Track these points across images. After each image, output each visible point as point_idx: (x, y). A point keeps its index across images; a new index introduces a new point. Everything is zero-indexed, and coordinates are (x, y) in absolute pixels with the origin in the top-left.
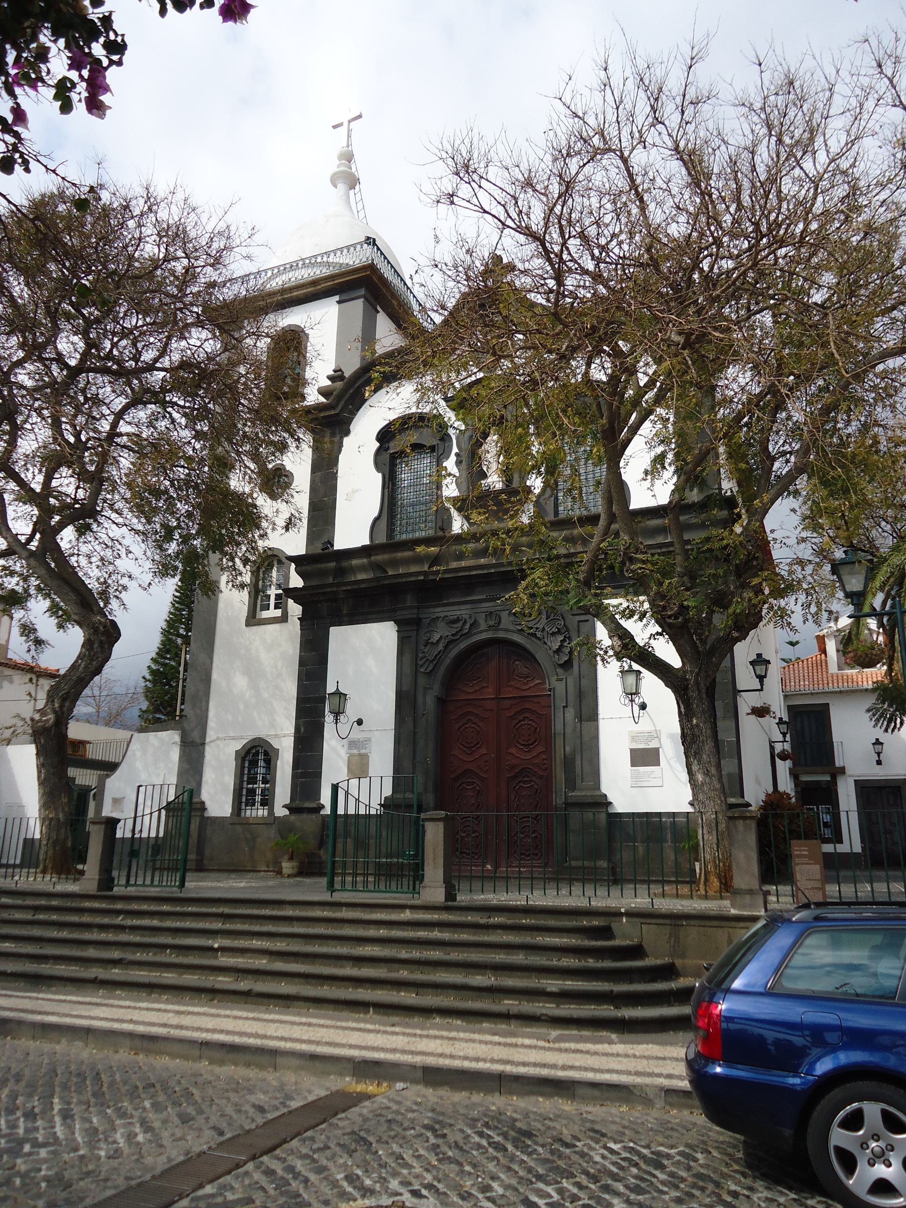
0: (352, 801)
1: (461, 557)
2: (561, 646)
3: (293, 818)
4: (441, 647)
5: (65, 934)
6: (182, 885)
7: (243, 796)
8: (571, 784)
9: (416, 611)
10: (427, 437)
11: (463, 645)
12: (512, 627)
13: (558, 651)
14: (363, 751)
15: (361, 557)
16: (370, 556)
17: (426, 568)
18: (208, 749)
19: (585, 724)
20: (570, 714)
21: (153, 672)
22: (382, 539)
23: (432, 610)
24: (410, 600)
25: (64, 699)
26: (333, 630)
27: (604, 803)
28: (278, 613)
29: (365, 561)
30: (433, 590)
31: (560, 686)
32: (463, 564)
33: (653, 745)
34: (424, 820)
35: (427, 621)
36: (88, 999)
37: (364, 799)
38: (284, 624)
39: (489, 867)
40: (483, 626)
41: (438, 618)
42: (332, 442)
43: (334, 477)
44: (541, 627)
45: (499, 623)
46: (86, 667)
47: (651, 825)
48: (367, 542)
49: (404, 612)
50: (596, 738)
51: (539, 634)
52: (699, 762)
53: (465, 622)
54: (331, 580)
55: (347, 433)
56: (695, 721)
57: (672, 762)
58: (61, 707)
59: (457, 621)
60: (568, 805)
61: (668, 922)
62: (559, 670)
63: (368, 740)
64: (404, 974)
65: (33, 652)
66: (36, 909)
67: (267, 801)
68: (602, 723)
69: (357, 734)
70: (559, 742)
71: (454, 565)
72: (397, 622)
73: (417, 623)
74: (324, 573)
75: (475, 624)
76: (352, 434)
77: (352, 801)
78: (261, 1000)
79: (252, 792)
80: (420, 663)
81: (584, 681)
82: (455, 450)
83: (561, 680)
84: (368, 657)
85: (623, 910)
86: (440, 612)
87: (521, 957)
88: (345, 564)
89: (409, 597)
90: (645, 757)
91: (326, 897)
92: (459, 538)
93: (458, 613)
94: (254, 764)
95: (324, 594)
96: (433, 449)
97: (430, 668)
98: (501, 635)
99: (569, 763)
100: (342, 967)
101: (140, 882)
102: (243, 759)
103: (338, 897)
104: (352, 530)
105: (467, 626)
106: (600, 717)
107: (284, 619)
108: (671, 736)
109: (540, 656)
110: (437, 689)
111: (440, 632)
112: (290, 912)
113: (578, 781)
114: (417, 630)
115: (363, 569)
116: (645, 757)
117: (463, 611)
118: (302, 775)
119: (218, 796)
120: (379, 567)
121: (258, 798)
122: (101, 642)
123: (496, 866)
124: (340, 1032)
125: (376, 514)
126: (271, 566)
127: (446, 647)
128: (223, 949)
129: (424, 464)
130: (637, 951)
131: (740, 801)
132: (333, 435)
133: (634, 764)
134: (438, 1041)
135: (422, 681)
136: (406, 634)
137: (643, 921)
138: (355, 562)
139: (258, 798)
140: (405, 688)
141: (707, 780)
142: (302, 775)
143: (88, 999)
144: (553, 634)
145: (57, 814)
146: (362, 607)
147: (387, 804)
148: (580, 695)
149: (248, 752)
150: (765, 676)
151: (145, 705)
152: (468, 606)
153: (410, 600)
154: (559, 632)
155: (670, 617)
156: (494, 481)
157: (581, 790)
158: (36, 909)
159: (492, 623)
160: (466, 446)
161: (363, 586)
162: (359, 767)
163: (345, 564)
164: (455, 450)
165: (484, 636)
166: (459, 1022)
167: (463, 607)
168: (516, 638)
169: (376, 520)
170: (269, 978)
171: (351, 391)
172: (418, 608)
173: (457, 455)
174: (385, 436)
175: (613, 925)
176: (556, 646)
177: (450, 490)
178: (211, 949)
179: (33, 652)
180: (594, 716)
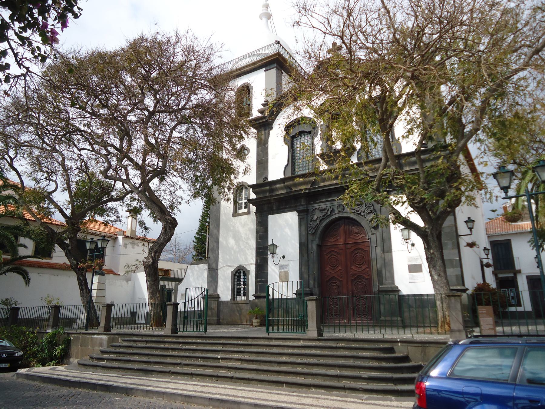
0: (275, 293)
1: (324, 180)
3: (257, 301)
4: (318, 221)
5: (158, 352)
6: (206, 331)
7: (235, 292)
8: (381, 282)
11: (328, 220)
14: (286, 270)
15: (281, 184)
16: (284, 183)
17: (309, 186)
18: (219, 271)
19: (386, 254)
20: (379, 249)
21: (197, 239)
22: (289, 175)
23: (313, 205)
24: (303, 202)
25: (155, 253)
26: (270, 217)
27: (396, 290)
28: (246, 210)
29: (282, 185)
30: (314, 196)
31: (373, 237)
32: (326, 184)
33: (419, 262)
34: (307, 300)
36: (166, 380)
37: (280, 291)
40: (337, 211)
44: (363, 210)
46: (164, 238)
47: (420, 301)
48: (283, 177)
49: (301, 207)
50: (391, 260)
51: (362, 214)
52: (435, 270)
53: (328, 210)
54: (268, 195)
55: (272, 128)
56: (432, 251)
58: (155, 256)
59: (325, 209)
60: (380, 292)
61: (420, 345)
62: (373, 230)
63: (288, 265)
64: (299, 369)
65: (144, 233)
66: (147, 342)
67: (246, 293)
68: (394, 254)
69: (283, 262)
70: (374, 263)
71: (322, 184)
73: (307, 211)
74: (264, 192)
75: (333, 211)
76: (274, 129)
77: (275, 293)
78: (237, 380)
79: (239, 290)
80: (309, 229)
81: (384, 234)
82: (320, 132)
83: (374, 234)
84: (286, 227)
85: (399, 340)
86: (317, 206)
87: (351, 362)
88: (273, 187)
89: (302, 200)
90: (414, 268)
91: (266, 335)
94: (239, 277)
95: (265, 201)
96: (309, 133)
97: (314, 231)
98: (345, 215)
99: (379, 273)
100: (272, 366)
101: (188, 330)
102: (235, 275)
103: (271, 335)
104: (276, 171)
105: (329, 212)
106: (393, 250)
107: (249, 213)
111: (317, 215)
112: (250, 342)
113: (384, 280)
115: (281, 188)
117: (327, 205)
118: (260, 282)
119: (225, 292)
121: (242, 292)
122: (170, 228)
124: (269, 395)
125: (286, 164)
126: (242, 189)
127: (320, 222)
128: (222, 359)
129: (306, 139)
130: (406, 359)
131: (462, 288)
132: (265, 130)
133: (410, 271)
134: (312, 399)
135: (310, 237)
136: (302, 217)
137: (409, 345)
138: (278, 186)
139: (242, 292)
140: (303, 241)
141: (440, 278)
142: (260, 282)
143: (166, 380)
144: (369, 213)
145: (155, 302)
146: (282, 204)
147: (298, 293)
148: (383, 240)
149: (236, 272)
150: (472, 228)
151: (194, 253)
152: (329, 203)
153: (303, 202)
154: (371, 212)
155: (416, 203)
157: (385, 284)
158: (147, 342)
159: (340, 210)
161: (282, 196)
162: (284, 277)
163: (273, 187)
164: (320, 132)
166: (323, 391)
167: (327, 203)
168: (352, 216)
169: (286, 166)
170: (241, 371)
174: (287, 128)
175: (395, 347)
177: (318, 150)
178: (217, 358)
179: (144, 233)
180: (390, 250)
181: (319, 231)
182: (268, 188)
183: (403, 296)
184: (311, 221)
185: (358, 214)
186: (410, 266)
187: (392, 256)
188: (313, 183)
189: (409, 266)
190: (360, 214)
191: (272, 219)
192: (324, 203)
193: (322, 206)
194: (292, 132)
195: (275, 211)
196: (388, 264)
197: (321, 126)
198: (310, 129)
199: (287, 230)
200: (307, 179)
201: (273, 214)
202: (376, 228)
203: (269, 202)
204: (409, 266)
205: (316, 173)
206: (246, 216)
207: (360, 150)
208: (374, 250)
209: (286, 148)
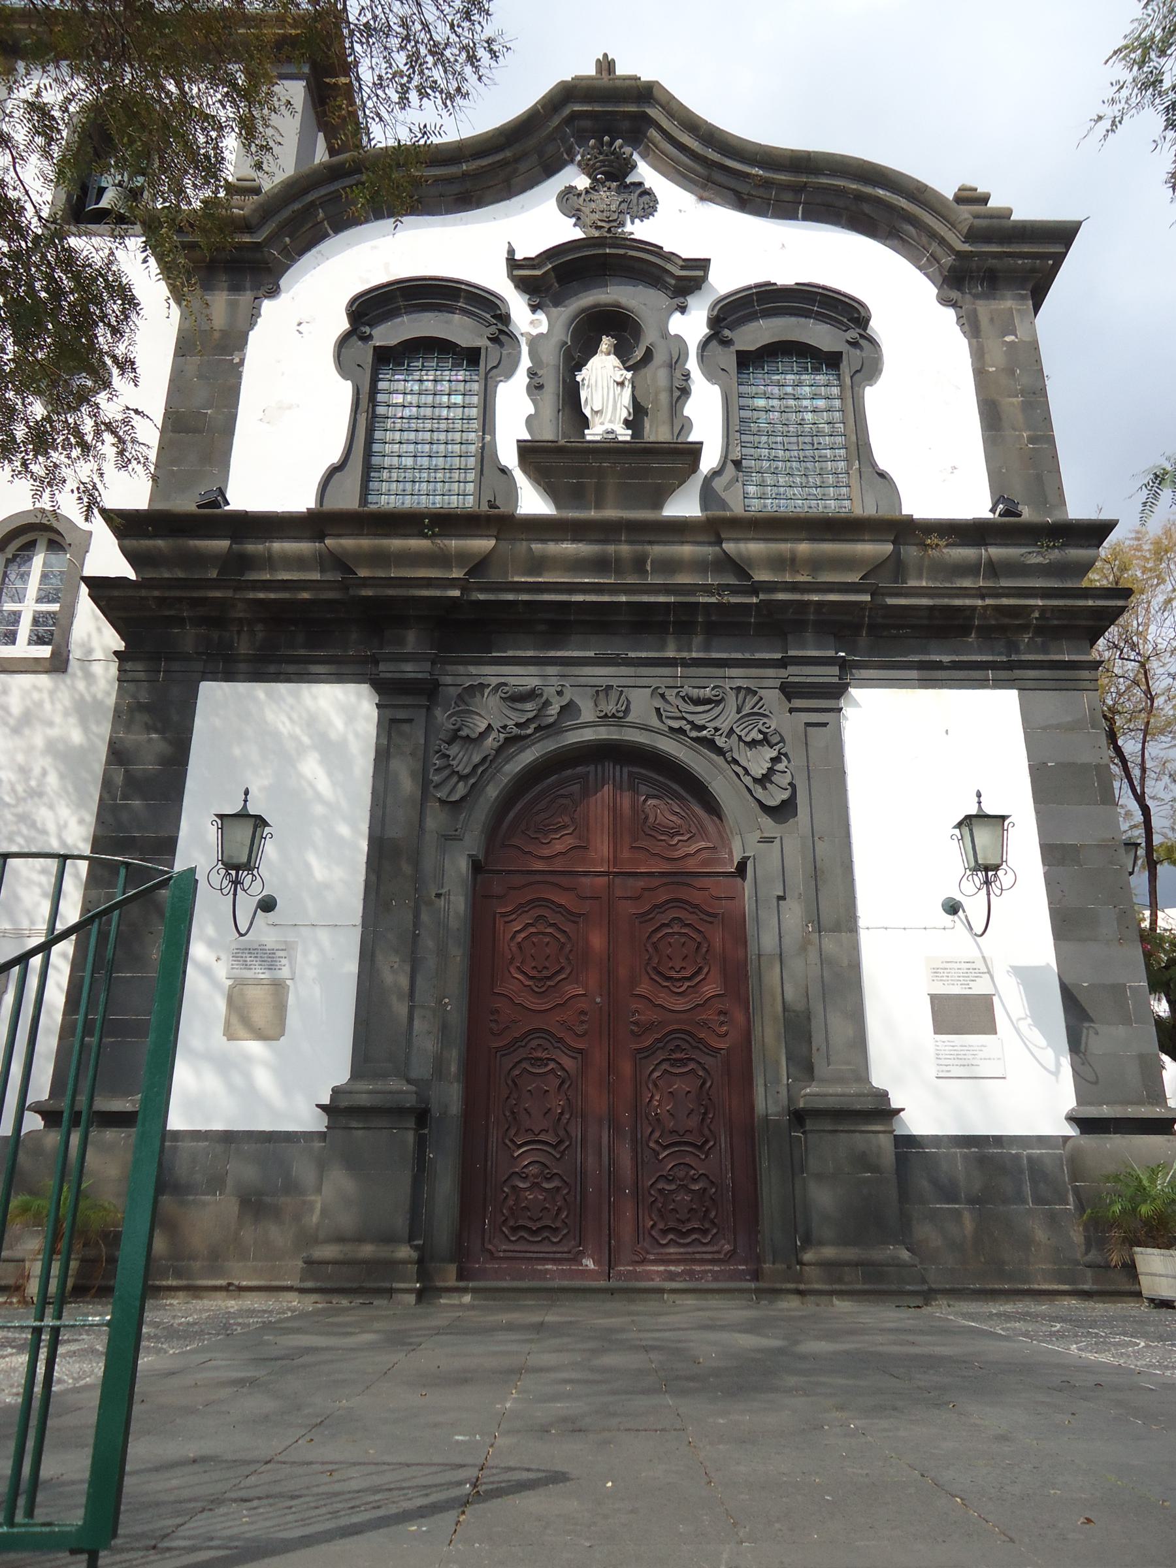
2: (771, 770)
3: (53, 1139)
8: (805, 1068)
9: (427, 666)
10: (459, 329)
12: (655, 722)
13: (764, 780)
16: (321, 537)
20: (793, 914)
23: (461, 669)
24: (412, 640)
26: (208, 689)
27: (882, 1111)
28: (45, 651)
30: (475, 624)
33: (980, 987)
35: (453, 692)
38: (62, 676)
39: (589, 1263)
40: (588, 713)
41: (482, 686)
42: (233, 305)
43: (235, 372)
44: (725, 727)
45: (627, 711)
50: (855, 966)
51: (720, 742)
53: (547, 703)
57: (1024, 1026)
59: (532, 695)
60: (799, 1117)
62: (766, 821)
63: (288, 947)
70: (772, 976)
72: (381, 686)
73: (428, 691)
75: (569, 709)
76: (284, 298)
80: (437, 779)
81: (820, 846)
82: (525, 362)
83: (769, 840)
84: (302, 754)
86: (491, 674)
88: (253, 548)
90: (961, 1014)
92: (536, 526)
93: (534, 682)
95: (195, 602)
97: (461, 790)
105: (554, 710)
106: (862, 923)
108: (1023, 974)
109: (720, 785)
110: (472, 842)
111: (490, 716)
114: (428, 708)
116: (961, 1014)
120: (339, 562)
123: (610, 1263)
125: (335, 457)
126: (30, 546)
127: (499, 750)
129: (447, 387)
132: (235, 288)
135: (435, 820)
136: (401, 714)
144: (753, 744)
148: (816, 875)
153: (412, 640)
154: (766, 741)
159: (610, 708)
160: (551, 356)
161: (305, 595)
163: (253, 548)
164: (525, 362)
168: (668, 746)
169: (334, 471)
171: (297, 206)
172: (433, 663)
173: (532, 373)
174: (369, 309)
176: (758, 770)
180: (847, 922)
181: (492, 792)
182: (224, 544)
183: (911, 1141)
184: (454, 737)
185: (696, 740)
186: (937, 1002)
187: (855, 948)
188: (480, 565)
189: (934, 998)
190: (710, 743)
191: (220, 705)
192: (532, 670)
193: (524, 678)
194: (388, 334)
196: (844, 982)
197: (534, 342)
198: (482, 342)
199: (312, 768)
201: (229, 677)
202: (783, 811)
203: (215, 618)
204: (934, 998)
205: (501, 522)
206: (44, 680)
207: (716, 473)
208: (769, 919)
209: (344, 390)
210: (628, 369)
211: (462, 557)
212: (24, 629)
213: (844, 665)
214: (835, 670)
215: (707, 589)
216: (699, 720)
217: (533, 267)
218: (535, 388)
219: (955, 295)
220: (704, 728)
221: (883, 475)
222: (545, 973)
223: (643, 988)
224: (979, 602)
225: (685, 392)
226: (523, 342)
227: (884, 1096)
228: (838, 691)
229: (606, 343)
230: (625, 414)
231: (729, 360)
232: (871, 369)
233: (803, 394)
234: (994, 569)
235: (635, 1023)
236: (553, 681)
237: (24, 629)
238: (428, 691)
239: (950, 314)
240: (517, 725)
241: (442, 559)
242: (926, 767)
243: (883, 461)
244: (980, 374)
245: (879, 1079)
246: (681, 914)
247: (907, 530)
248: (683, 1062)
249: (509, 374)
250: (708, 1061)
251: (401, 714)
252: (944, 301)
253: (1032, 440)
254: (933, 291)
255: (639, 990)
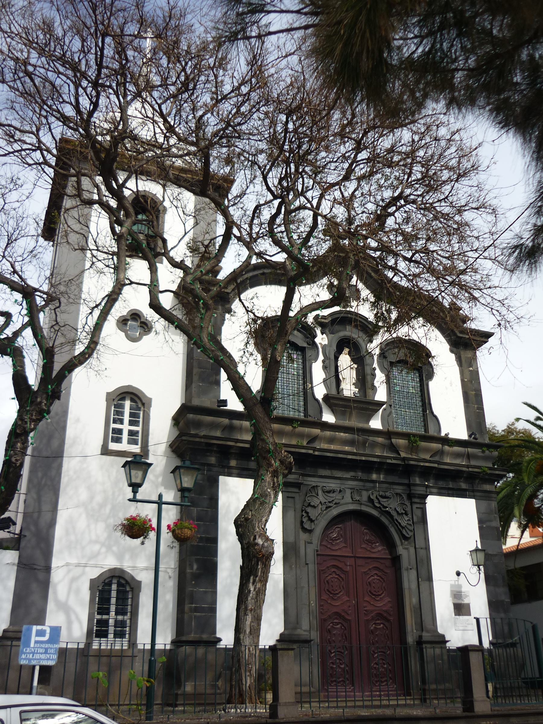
1: (331, 440)
11: (335, 512)
17: (305, 443)
20: (413, 573)
26: (222, 479)
27: (442, 640)
32: (332, 447)
71: (325, 446)
82: (321, 357)
117: (333, 485)
135: (304, 536)
136: (290, 495)
139: (111, 630)
140: (291, 539)
156: (349, 389)
159: (358, 498)
165: (352, 507)
173: (323, 362)
180: (430, 579)
182: (226, 421)
184: (309, 505)
188: (313, 439)
195: (235, 471)
197: (324, 347)
198: (305, 345)
200: (306, 430)
210: (355, 363)
211: (308, 435)
212: (125, 436)
213: (427, 487)
214: (424, 489)
215: (390, 458)
216: (385, 505)
217: (325, 319)
218: (325, 368)
219: (455, 349)
220: (387, 507)
221: (436, 417)
222: (337, 592)
223: (367, 598)
224: (467, 470)
225: (374, 376)
226: (319, 346)
227: (443, 636)
228: (425, 497)
229: (346, 350)
230: (354, 381)
231: (386, 365)
232: (431, 375)
233: (408, 381)
234: (469, 456)
235: (366, 611)
236: (338, 485)
237: (125, 436)
238: (298, 485)
239: (453, 356)
240: (330, 502)
241: (301, 436)
242: (452, 525)
243: (435, 413)
244: (462, 381)
245: (440, 631)
246: (380, 574)
247: (446, 441)
248: (380, 624)
249: (316, 360)
250: (386, 624)
251: (290, 495)
252: (452, 351)
253: (478, 408)
254: (449, 347)
255: (365, 599)
